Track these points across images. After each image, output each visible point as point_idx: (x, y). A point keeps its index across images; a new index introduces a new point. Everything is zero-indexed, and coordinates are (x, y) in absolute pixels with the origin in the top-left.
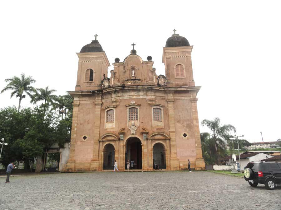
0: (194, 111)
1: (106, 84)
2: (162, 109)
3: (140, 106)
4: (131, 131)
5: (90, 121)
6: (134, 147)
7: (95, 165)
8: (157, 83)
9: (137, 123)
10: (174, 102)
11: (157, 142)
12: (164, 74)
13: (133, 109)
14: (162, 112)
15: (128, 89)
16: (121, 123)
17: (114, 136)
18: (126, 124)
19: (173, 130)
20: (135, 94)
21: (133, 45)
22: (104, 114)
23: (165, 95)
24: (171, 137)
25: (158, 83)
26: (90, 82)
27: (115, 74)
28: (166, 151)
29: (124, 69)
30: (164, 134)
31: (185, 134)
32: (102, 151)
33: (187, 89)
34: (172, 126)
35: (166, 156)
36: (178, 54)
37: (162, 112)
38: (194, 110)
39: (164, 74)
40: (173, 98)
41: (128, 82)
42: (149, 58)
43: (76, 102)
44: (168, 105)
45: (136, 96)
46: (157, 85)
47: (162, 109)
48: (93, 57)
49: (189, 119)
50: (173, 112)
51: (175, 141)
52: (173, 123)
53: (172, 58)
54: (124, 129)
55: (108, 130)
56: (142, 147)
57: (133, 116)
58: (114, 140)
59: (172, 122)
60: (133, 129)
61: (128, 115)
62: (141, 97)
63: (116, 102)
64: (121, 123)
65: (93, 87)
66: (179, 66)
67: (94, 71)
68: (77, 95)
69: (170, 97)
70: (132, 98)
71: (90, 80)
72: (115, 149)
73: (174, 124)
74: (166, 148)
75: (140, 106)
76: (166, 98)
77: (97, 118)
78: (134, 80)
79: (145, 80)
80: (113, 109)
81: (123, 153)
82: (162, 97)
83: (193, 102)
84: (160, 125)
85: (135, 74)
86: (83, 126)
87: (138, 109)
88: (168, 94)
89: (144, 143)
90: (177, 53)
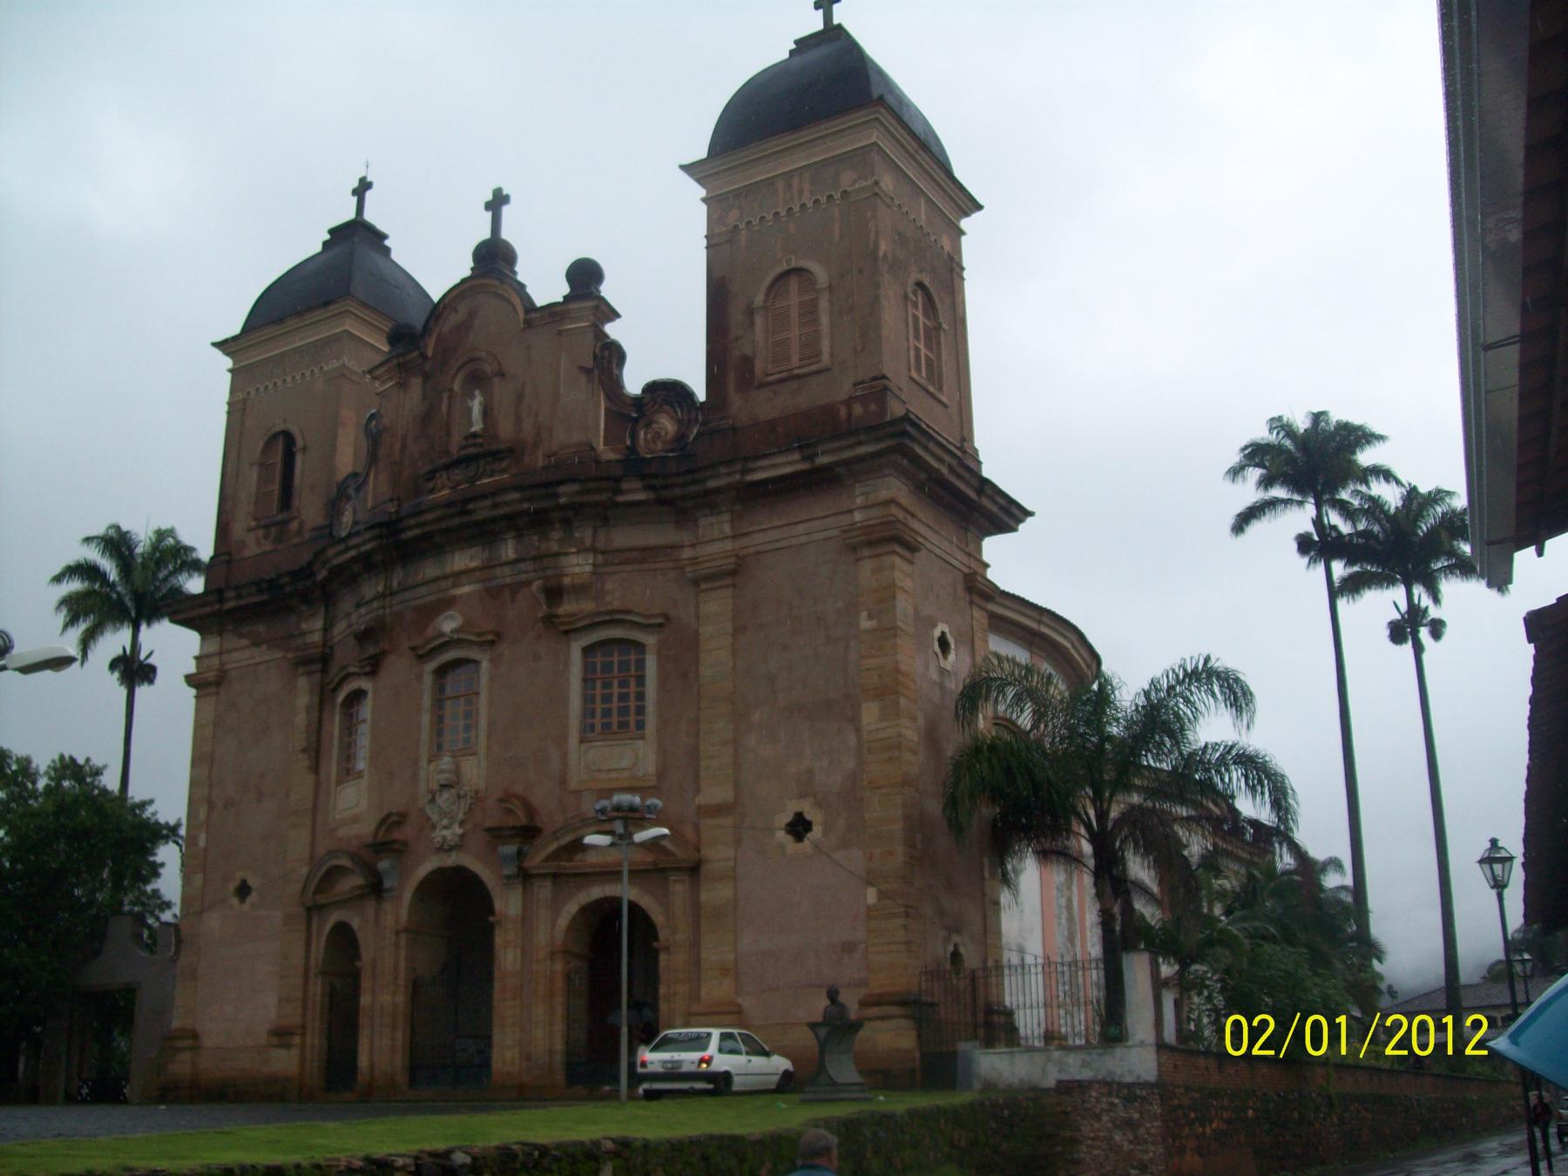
2: (650, 640)
3: (492, 643)
4: (434, 827)
7: (285, 1062)
9: (475, 772)
10: (735, 572)
11: (597, 892)
12: (691, 370)
18: (415, 776)
19: (715, 792)
20: (472, 559)
21: (497, 203)
23: (685, 537)
24: (706, 852)
28: (663, 957)
35: (663, 990)
36: (790, 187)
38: (870, 617)
39: (691, 370)
40: (728, 545)
42: (585, 276)
44: (697, 607)
48: (299, 351)
53: (743, 236)
54: (403, 816)
56: (497, 932)
60: (443, 814)
61: (426, 719)
66: (794, 283)
67: (299, 443)
68: (208, 616)
69: (715, 538)
74: (663, 934)
75: (492, 641)
76: (687, 553)
81: (396, 978)
83: (866, 552)
84: (624, 763)
85: (487, 413)
87: (485, 665)
88: (702, 522)
89: (508, 903)
90: (781, 185)
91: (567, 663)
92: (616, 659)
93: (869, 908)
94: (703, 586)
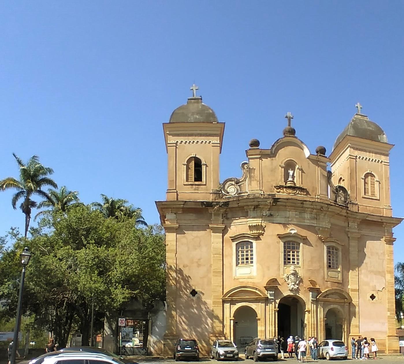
1: (232, 190)
5: (201, 260)
6: (289, 315)
11: (332, 306)
13: (291, 245)
14: (340, 254)
15: (284, 204)
16: (268, 268)
17: (257, 291)
22: (229, 249)
27: (253, 171)
30: (343, 294)
32: (230, 320)
37: (340, 254)
41: (281, 191)
44: (349, 243)
47: (340, 248)
55: (241, 280)
58: (257, 301)
63: (257, 227)
64: (268, 268)
65: (203, 194)
72: (258, 315)
76: (347, 230)
77: (215, 256)
80: (250, 240)
93: (388, 316)
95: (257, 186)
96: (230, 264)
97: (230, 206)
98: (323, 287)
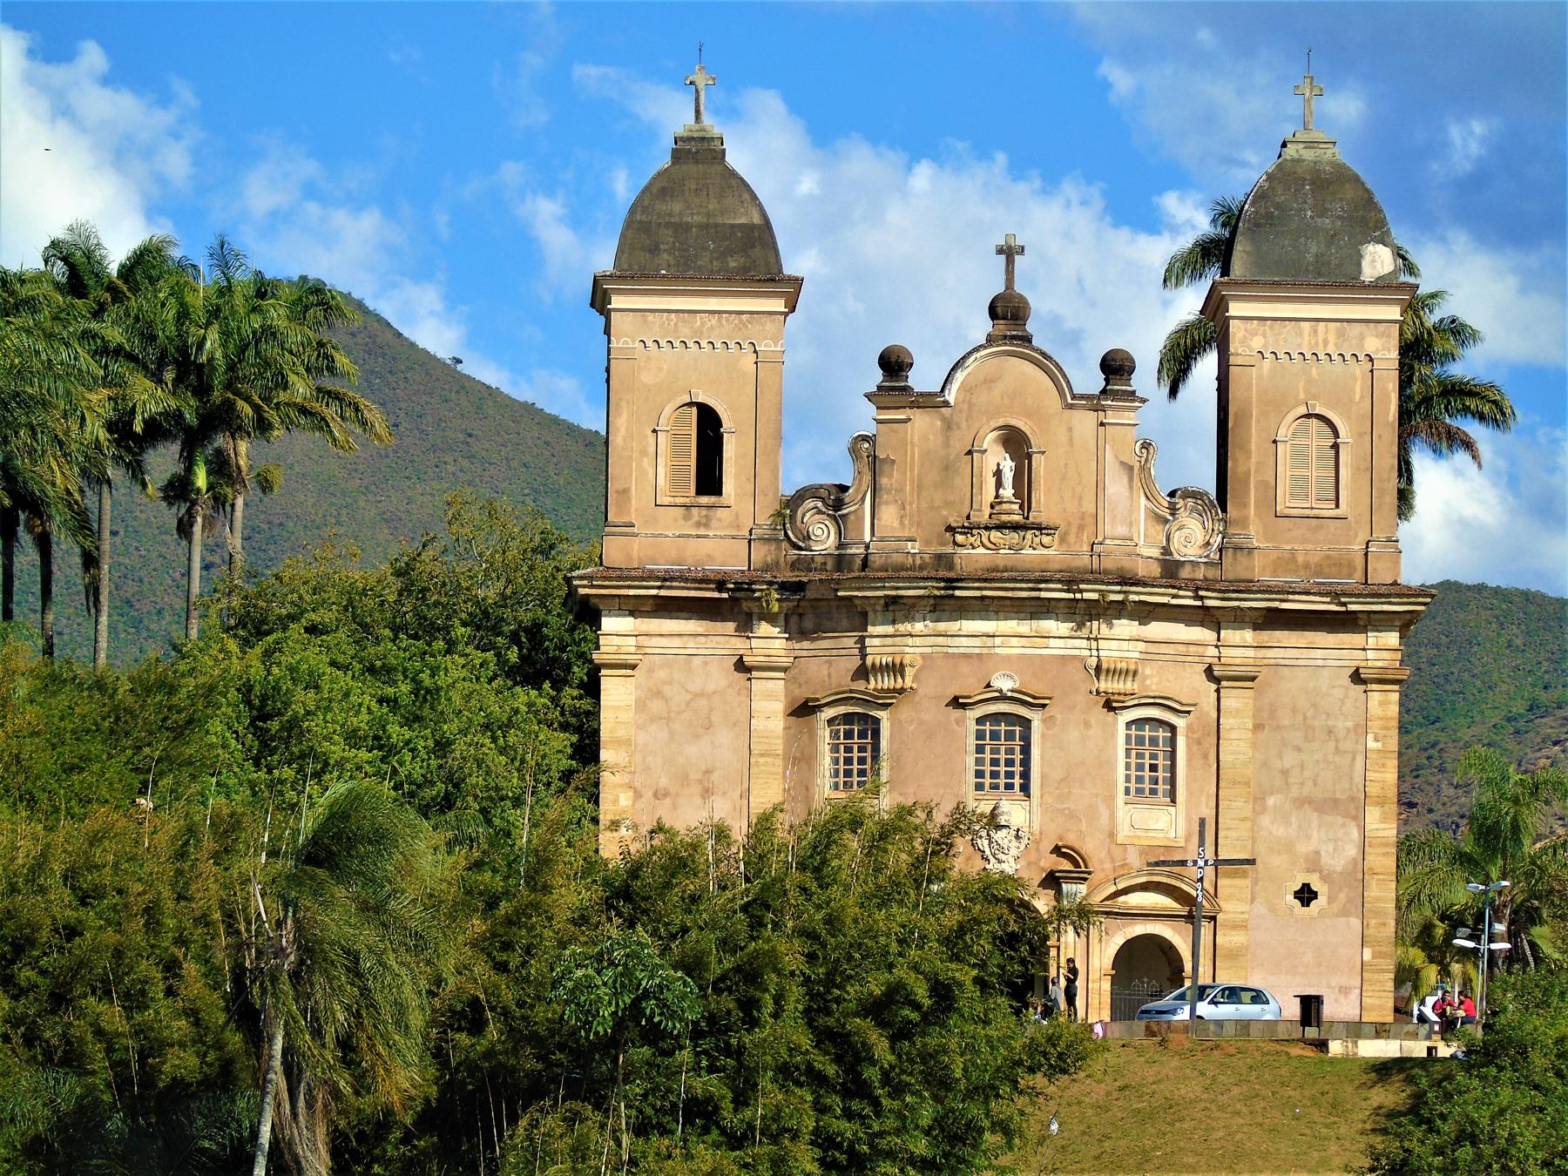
0: (1378, 745)
5: (715, 777)
8: (1156, 553)
15: (977, 593)
21: (1009, 253)
22: (805, 738)
25: (1166, 551)
26: (704, 500)
27: (886, 467)
29: (947, 444)
30: (1184, 887)
31: (1306, 887)
33: (1344, 604)
34: (1233, 834)
38: (1376, 740)
43: (616, 641)
45: (1024, 641)
46: (1156, 570)
49: (1338, 796)
50: (1243, 747)
51: (1242, 926)
52: (1243, 820)
57: (1002, 769)
59: (1235, 807)
62: (1056, 648)
67: (727, 424)
70: (997, 650)
71: (699, 492)
73: (1248, 824)
78: (1015, 527)
79: (1081, 528)
82: (1182, 649)
86: (675, 807)
91: (1114, 734)
92: (1147, 733)
94: (1224, 683)
95: (896, 524)
96: (807, 789)
97: (810, 594)
98: (1108, 866)
